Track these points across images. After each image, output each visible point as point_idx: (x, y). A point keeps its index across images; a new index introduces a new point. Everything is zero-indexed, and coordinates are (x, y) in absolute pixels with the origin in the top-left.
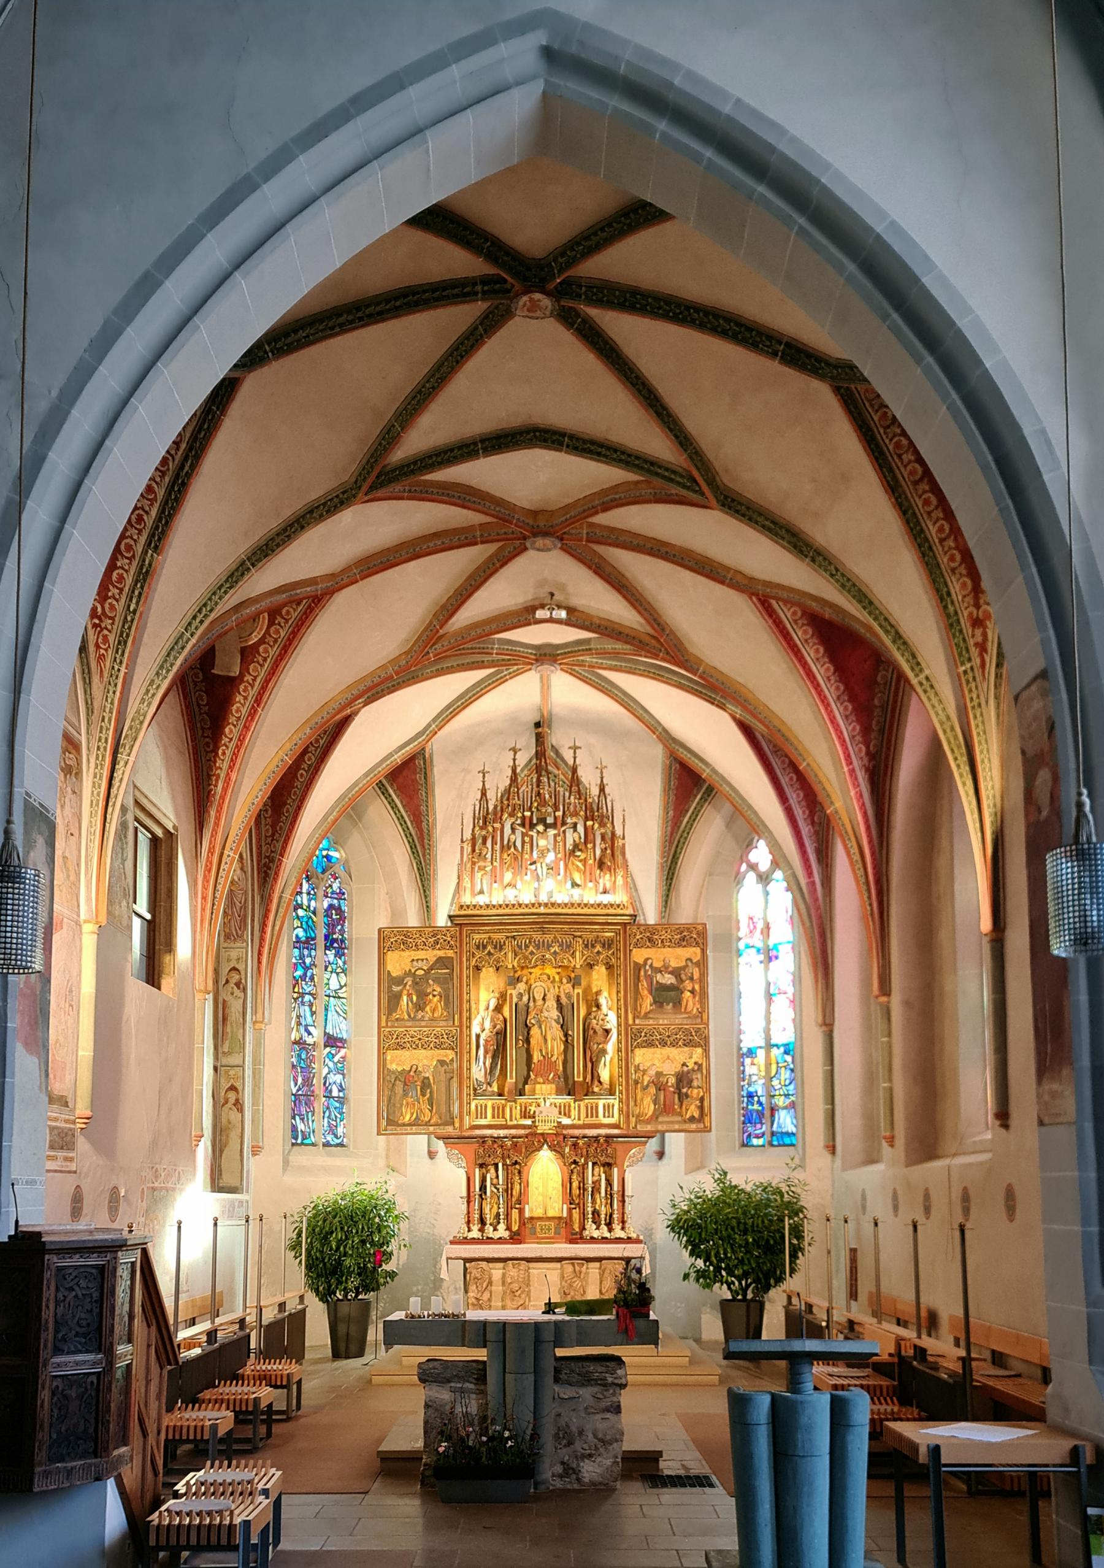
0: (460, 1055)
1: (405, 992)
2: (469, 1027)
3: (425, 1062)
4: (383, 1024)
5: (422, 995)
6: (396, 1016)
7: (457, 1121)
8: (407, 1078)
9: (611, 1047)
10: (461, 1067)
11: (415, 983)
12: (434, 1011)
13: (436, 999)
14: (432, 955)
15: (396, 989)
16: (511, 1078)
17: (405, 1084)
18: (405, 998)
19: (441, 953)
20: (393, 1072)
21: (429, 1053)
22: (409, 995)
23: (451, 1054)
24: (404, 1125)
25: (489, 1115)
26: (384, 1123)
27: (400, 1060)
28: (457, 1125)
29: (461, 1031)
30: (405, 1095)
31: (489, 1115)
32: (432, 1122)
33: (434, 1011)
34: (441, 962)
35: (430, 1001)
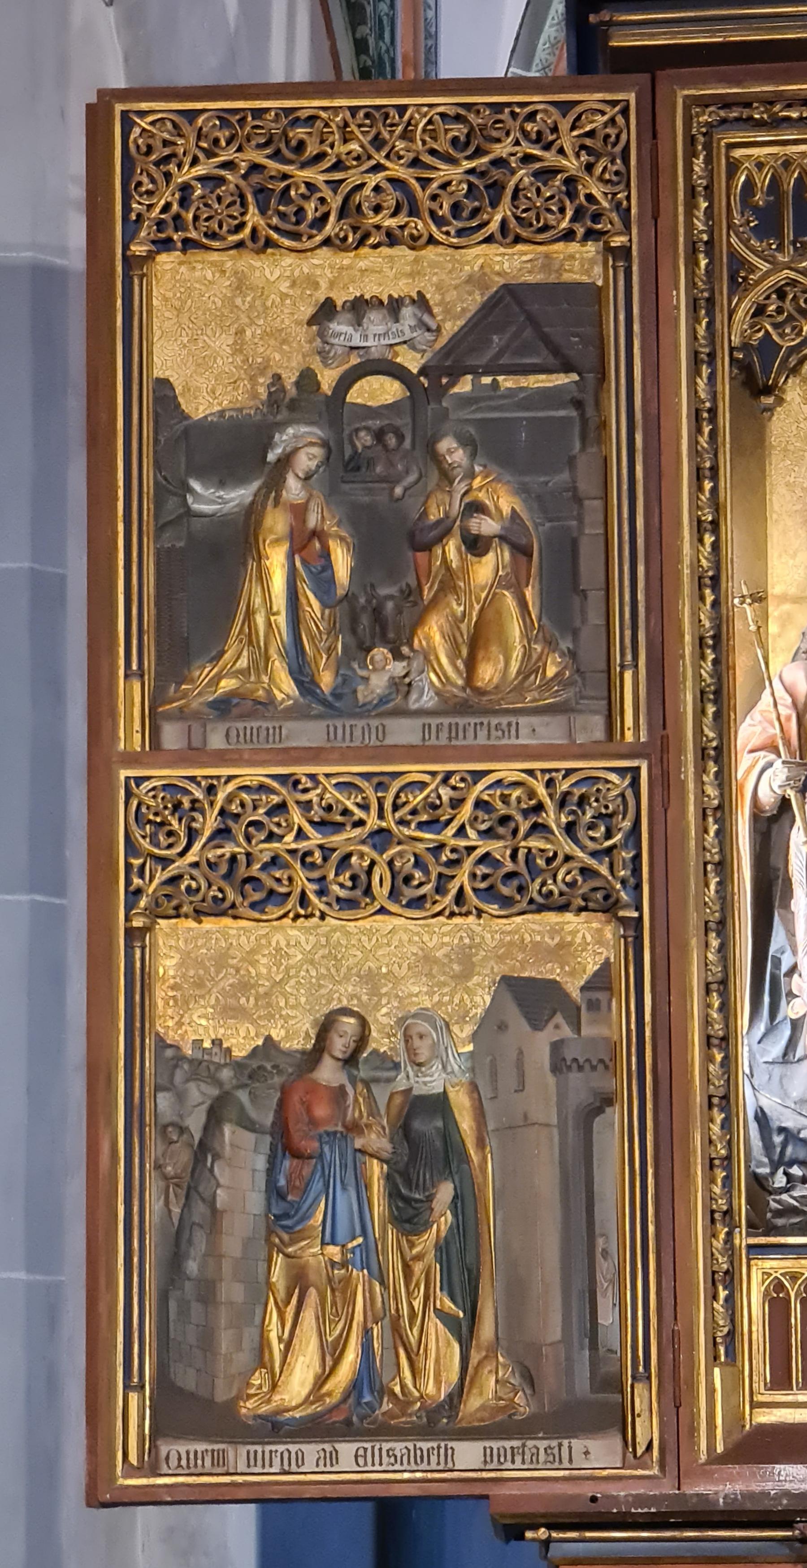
0: (650, 944)
1: (277, 522)
2: (719, 755)
3: (419, 994)
4: (130, 735)
5: (396, 543)
6: (218, 677)
7: (644, 1400)
8: (291, 1103)
10: (668, 1031)
11: (344, 467)
12: (474, 644)
13: (485, 570)
14: (457, 275)
15: (211, 499)
17: (283, 1144)
18: (277, 562)
19: (513, 263)
20: (201, 1067)
21: (442, 934)
22: (305, 542)
23: (586, 943)
24: (275, 1428)
26: (134, 1412)
27: (237, 985)
28: (647, 1429)
29: (665, 782)
30: (283, 1214)
32: (473, 1403)
33: (474, 644)
34: (515, 320)
35: (449, 583)
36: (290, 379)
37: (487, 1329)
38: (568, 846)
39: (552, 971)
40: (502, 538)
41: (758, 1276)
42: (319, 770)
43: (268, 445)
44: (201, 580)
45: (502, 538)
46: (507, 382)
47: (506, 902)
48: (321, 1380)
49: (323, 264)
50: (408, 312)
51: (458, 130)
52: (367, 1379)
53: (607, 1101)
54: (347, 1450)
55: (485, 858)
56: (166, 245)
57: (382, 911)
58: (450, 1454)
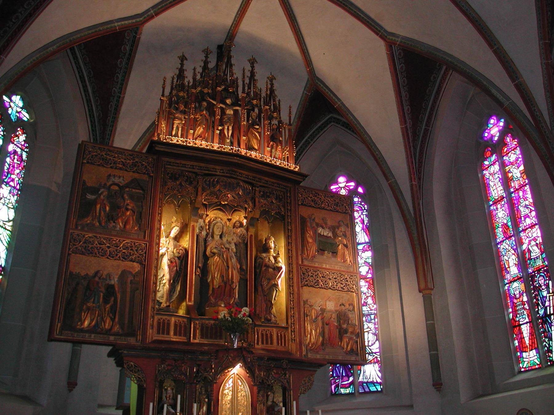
5: (115, 207)
7: (139, 333)
9: (281, 282)
14: (129, 176)
15: (90, 197)
16: (190, 300)
21: (116, 263)
25: (172, 333)
28: (140, 337)
31: (172, 333)
32: (113, 331)
36: (103, 183)
37: (117, 320)
38: (136, 253)
39: (131, 270)
40: (131, 210)
41: (156, 318)
42: (101, 236)
43: (99, 191)
44: (86, 208)
45: (131, 210)
46: (134, 190)
47: (125, 259)
48: (90, 324)
49: (110, 171)
50: (122, 178)
51: (132, 157)
52: (97, 324)
53: (137, 289)
54: (93, 335)
55: (124, 252)
56: (88, 163)
57: (107, 258)
58: (109, 338)
